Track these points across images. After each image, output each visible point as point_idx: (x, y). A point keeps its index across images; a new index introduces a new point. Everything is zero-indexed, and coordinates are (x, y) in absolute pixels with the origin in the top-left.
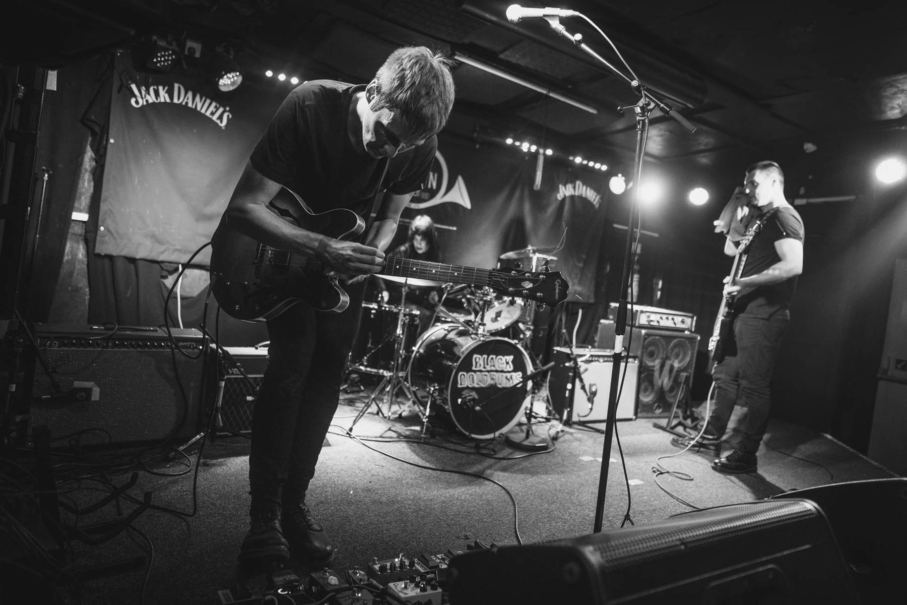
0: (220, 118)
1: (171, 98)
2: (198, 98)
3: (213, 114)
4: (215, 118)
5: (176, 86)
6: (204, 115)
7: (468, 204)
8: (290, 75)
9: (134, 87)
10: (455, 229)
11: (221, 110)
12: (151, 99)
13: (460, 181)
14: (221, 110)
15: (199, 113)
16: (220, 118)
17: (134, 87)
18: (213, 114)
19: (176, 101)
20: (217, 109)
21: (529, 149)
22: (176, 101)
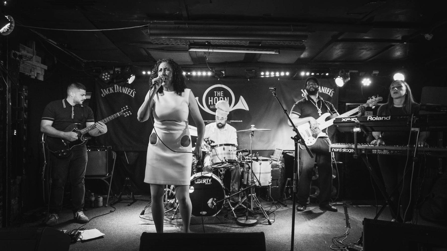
0: (132, 94)
1: (114, 90)
2: (123, 89)
3: (129, 93)
4: (130, 94)
5: (115, 85)
6: (126, 94)
7: (247, 108)
8: (146, 71)
9: (102, 90)
10: (242, 121)
11: (132, 91)
12: (107, 92)
13: (241, 97)
14: (132, 91)
15: (124, 93)
16: (132, 94)
17: (102, 90)
18: (129, 93)
19: (116, 91)
20: (130, 91)
21: (270, 75)
22: (116, 91)
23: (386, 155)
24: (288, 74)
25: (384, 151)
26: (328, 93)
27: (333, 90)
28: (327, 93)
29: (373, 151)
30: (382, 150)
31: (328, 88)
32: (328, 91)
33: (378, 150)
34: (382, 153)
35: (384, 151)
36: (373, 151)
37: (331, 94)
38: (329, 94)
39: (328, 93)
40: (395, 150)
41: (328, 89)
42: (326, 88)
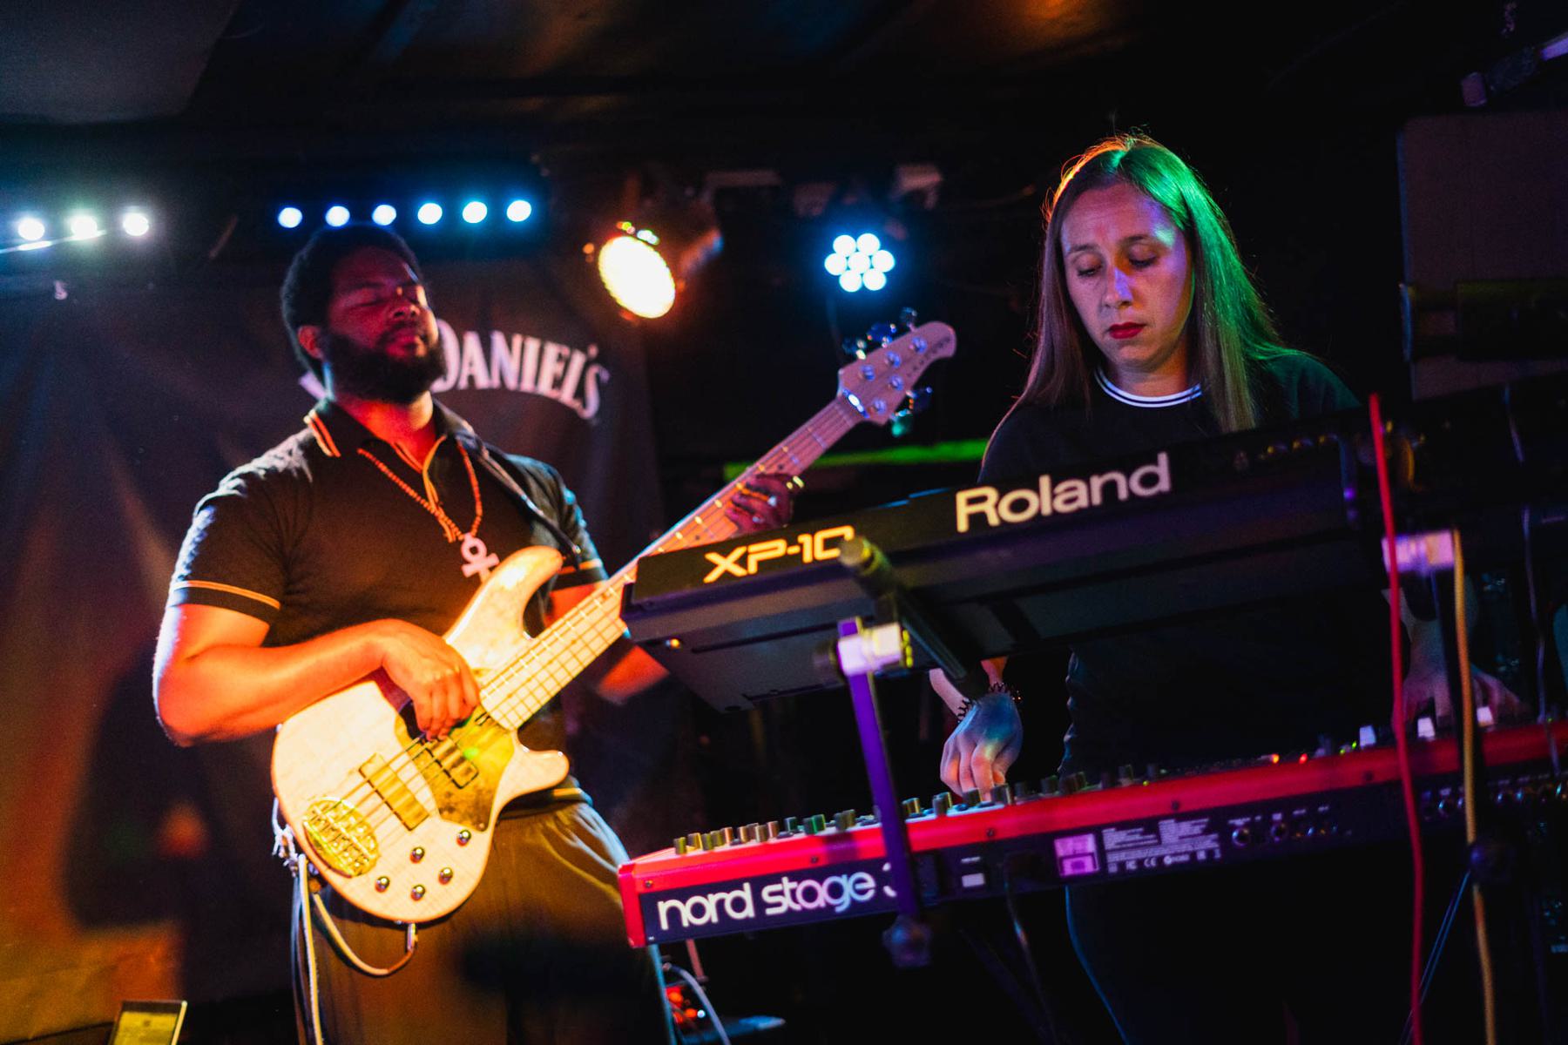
23: (1190, 870)
24: (138, 223)
25: (1171, 830)
26: (558, 383)
27: (600, 360)
28: (545, 387)
29: (1063, 847)
30: (1151, 826)
31: (545, 336)
32: (551, 367)
33: (1112, 838)
34: (1150, 855)
35: (1171, 830)
36: (1063, 847)
37: (580, 393)
38: (566, 395)
39: (558, 383)
40: (1268, 807)
41: (552, 350)
42: (533, 345)
